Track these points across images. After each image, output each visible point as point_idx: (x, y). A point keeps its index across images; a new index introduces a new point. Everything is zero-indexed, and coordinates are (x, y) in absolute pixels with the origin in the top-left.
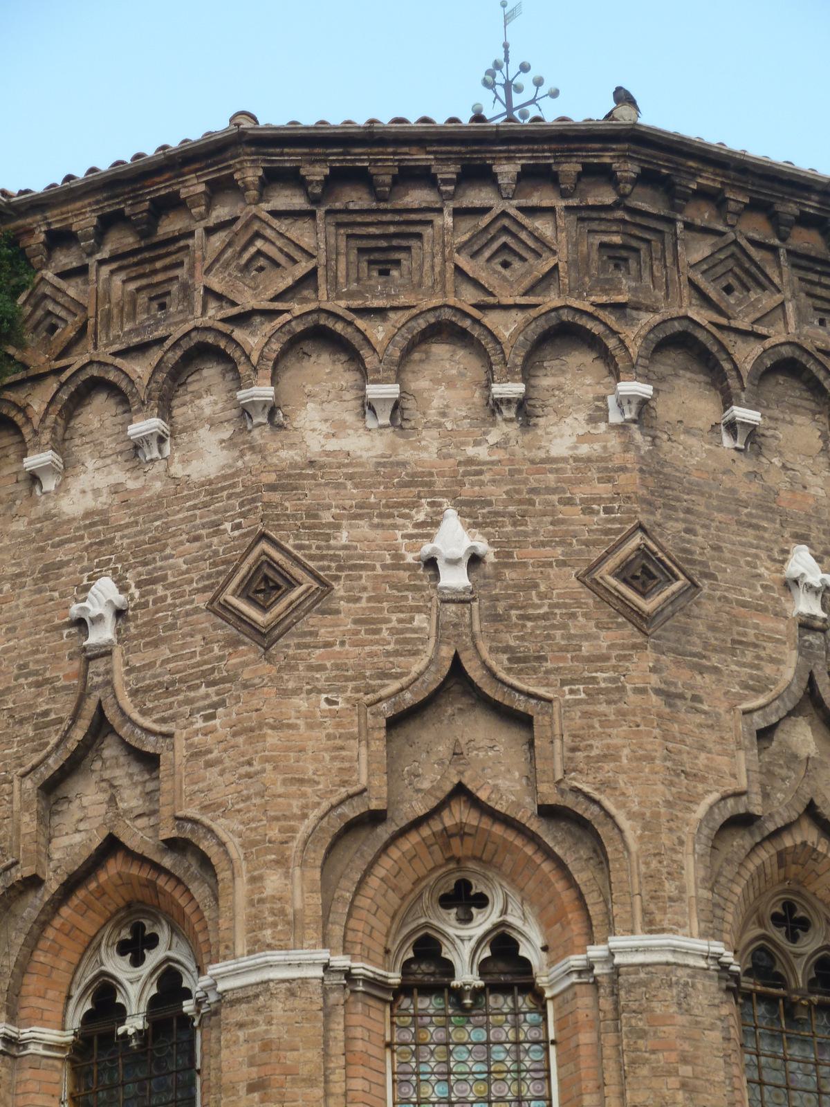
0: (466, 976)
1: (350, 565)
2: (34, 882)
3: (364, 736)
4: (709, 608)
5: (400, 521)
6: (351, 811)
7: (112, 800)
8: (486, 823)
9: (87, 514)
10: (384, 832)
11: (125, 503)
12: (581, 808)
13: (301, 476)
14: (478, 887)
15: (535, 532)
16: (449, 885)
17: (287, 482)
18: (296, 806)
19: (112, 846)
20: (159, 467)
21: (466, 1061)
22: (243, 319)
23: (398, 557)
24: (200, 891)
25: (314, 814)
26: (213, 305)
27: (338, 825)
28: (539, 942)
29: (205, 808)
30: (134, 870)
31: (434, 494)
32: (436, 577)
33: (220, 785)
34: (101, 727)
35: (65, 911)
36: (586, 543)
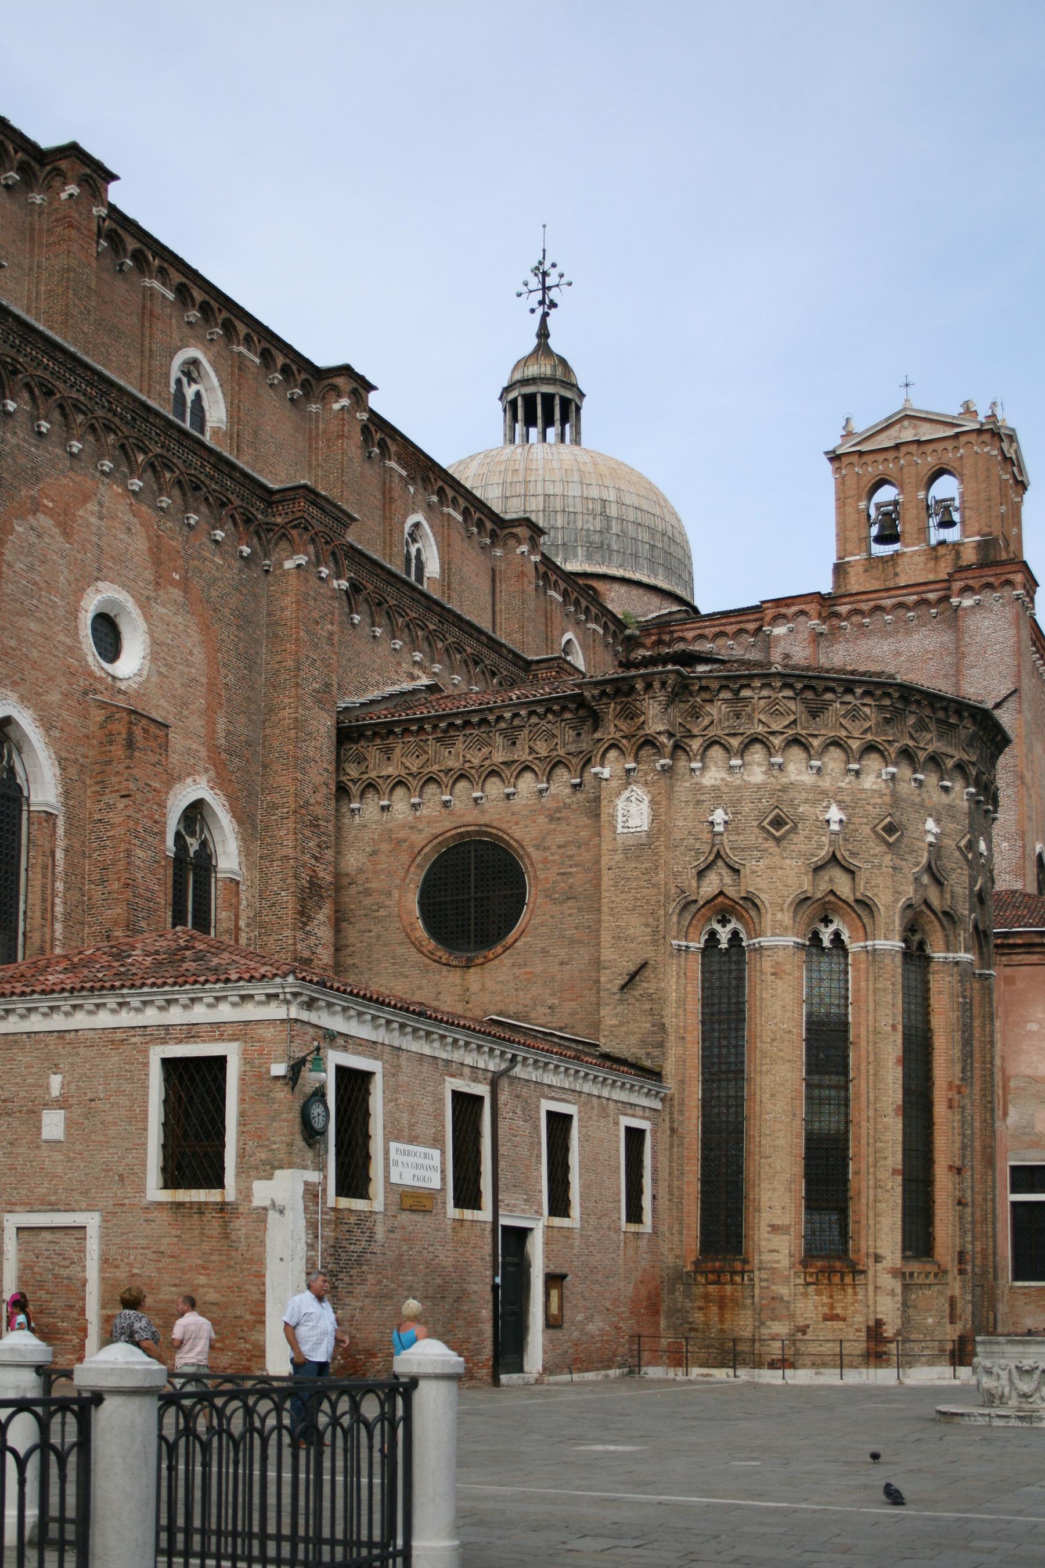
0: (826, 943)
2: (696, 901)
3: (806, 874)
6: (802, 897)
7: (721, 880)
8: (837, 901)
9: (712, 786)
10: (809, 902)
12: (868, 901)
14: (830, 917)
16: (822, 916)
17: (784, 789)
18: (786, 893)
19: (721, 893)
20: (739, 776)
21: (824, 967)
22: (773, 733)
24: (753, 913)
25: (792, 897)
26: (761, 725)
27: (798, 900)
28: (848, 935)
29: (756, 889)
30: (727, 901)
33: (762, 883)
34: (718, 855)
35: (703, 910)
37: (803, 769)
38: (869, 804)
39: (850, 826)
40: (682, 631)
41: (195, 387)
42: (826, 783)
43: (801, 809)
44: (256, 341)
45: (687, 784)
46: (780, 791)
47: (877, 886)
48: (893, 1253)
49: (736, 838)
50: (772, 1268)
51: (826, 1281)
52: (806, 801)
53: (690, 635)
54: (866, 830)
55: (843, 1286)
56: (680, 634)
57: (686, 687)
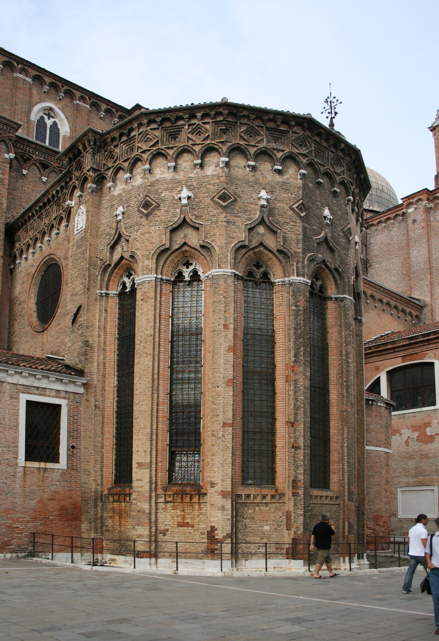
1: (164, 200)
4: (239, 204)
5: (175, 191)
11: (125, 192)
13: (155, 183)
15: (202, 191)
17: (152, 185)
23: (174, 198)
31: (182, 185)
32: (181, 201)
36: (213, 192)
37: (166, 170)
38: (210, 184)
39: (196, 200)
40: (372, 221)
41: (52, 120)
42: (180, 176)
43: (163, 195)
44: (88, 99)
45: (108, 198)
46: (149, 186)
47: (214, 235)
48: (222, 480)
49: (128, 221)
50: (138, 491)
51: (179, 500)
52: (167, 189)
53: (375, 222)
54: (208, 201)
55: (191, 504)
56: (371, 223)
57: (105, 141)
